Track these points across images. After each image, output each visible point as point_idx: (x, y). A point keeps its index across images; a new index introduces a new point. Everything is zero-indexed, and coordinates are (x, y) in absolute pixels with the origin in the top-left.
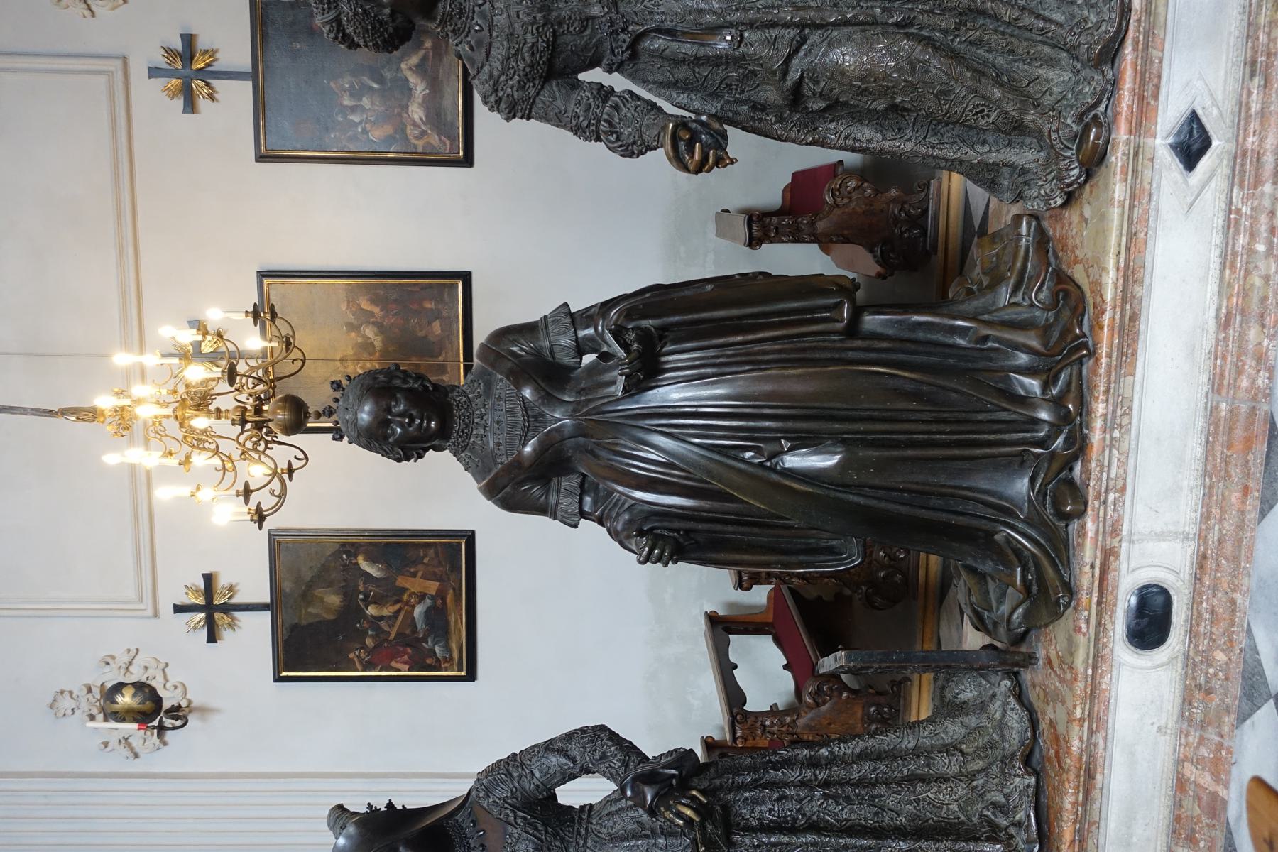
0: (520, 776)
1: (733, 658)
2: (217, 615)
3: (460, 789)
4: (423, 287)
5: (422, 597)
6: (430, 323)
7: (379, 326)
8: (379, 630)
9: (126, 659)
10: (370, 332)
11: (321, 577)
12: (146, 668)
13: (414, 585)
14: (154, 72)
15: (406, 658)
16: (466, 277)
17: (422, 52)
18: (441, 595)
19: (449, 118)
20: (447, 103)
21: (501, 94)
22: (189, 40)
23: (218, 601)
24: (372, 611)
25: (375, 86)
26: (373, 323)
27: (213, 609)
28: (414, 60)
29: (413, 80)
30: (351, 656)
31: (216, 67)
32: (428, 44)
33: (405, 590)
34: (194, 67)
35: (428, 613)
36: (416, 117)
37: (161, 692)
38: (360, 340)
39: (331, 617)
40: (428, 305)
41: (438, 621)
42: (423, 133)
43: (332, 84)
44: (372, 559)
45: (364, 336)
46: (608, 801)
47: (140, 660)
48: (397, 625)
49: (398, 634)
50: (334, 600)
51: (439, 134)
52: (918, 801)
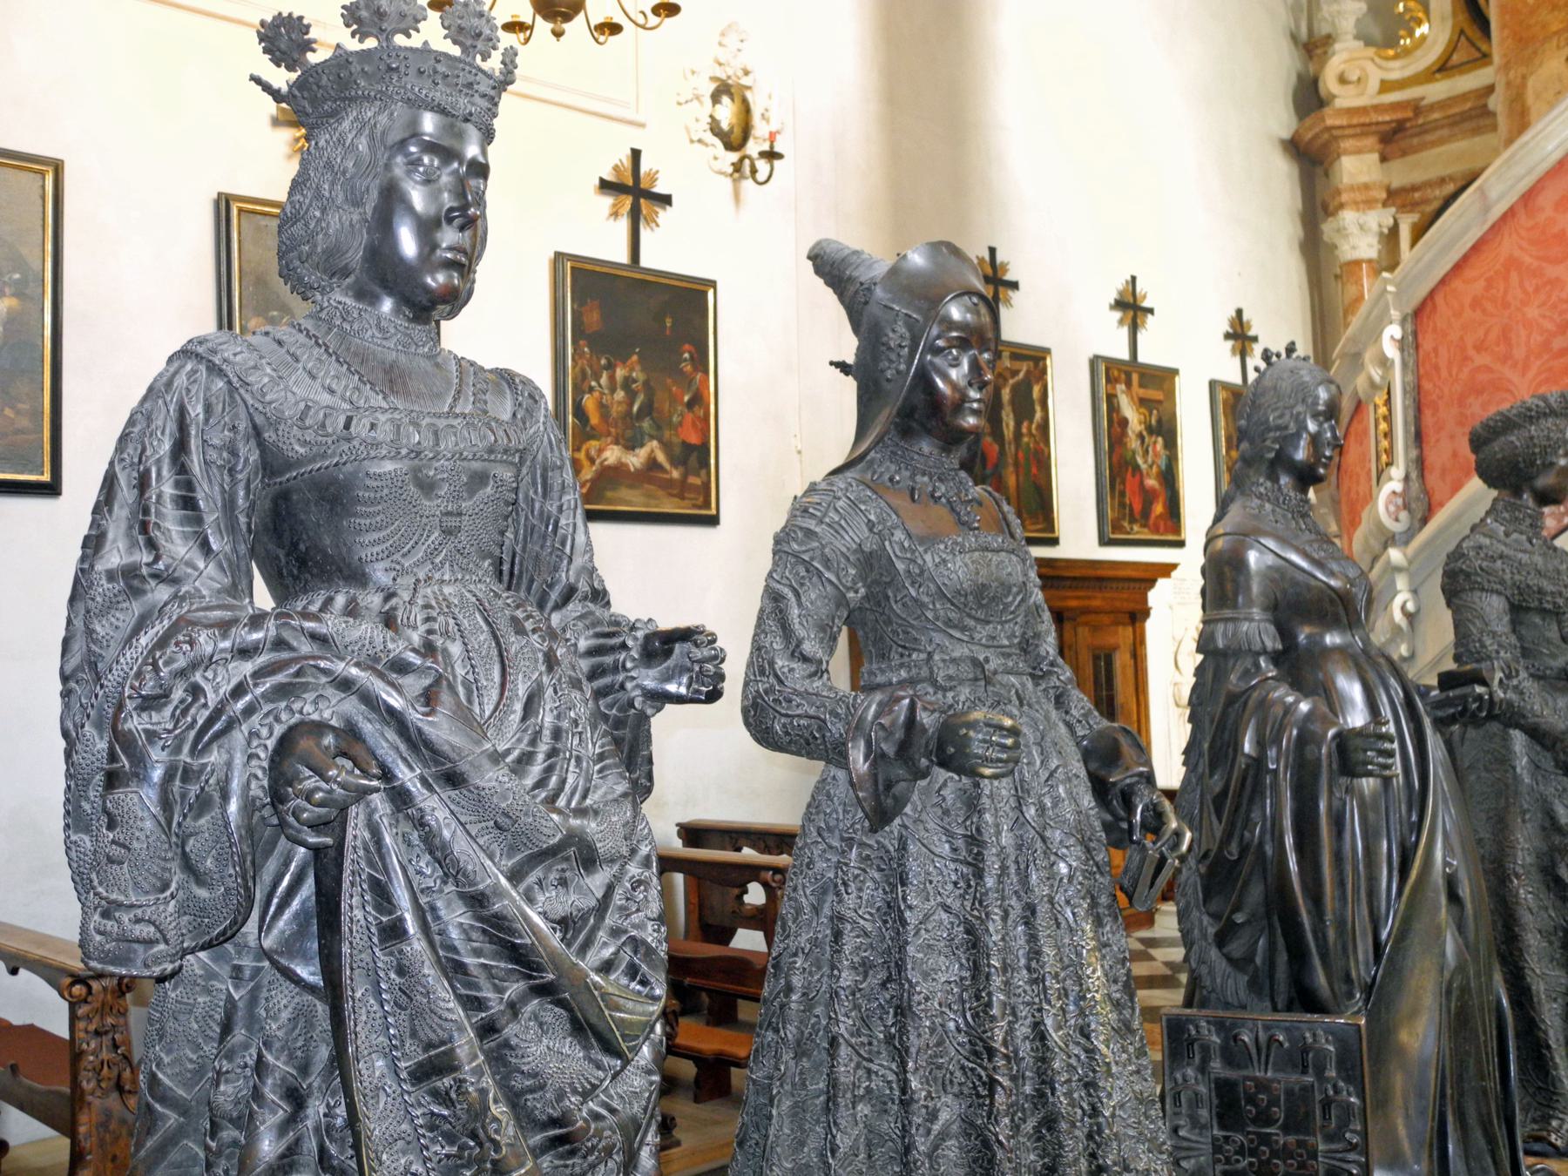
14: (636, 154)
17: (667, 466)
19: (609, 494)
20: (624, 493)
21: (1499, 563)
25: (635, 408)
28: (661, 457)
29: (643, 453)
32: (676, 474)
43: (635, 358)
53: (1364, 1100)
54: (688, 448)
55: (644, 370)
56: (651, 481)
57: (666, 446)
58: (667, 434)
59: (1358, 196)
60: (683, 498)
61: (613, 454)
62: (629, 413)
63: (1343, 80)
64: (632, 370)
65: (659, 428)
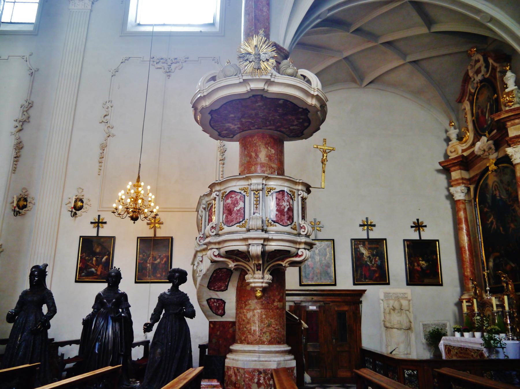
1: (73, 345)
3: (48, 287)
5: (96, 270)
8: (90, 260)
10: (158, 260)
11: (103, 248)
13: (100, 269)
18: (96, 275)
23: (100, 225)
24: (94, 259)
27: (98, 223)
33: (99, 266)
35: (93, 272)
39: (94, 249)
40: (164, 274)
41: (91, 274)
44: (106, 259)
46: (43, 313)
49: (88, 265)
50: (98, 250)
59: (455, 183)
63: (451, 152)
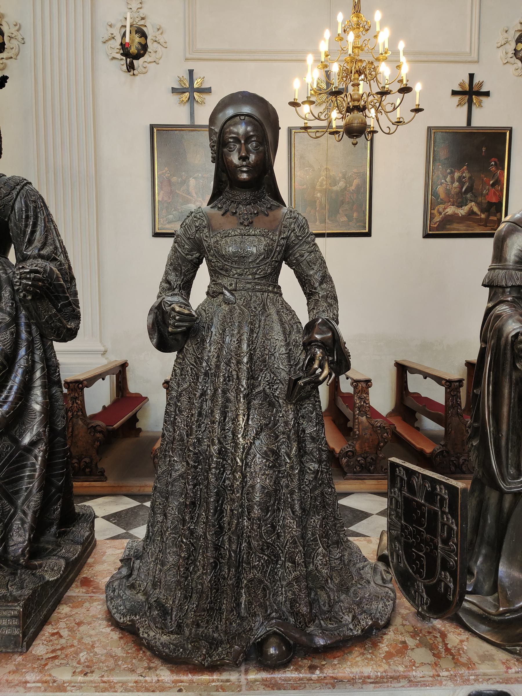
0: (309, 243)
2: (187, 94)
4: (364, 212)
6: (346, 215)
7: (345, 189)
9: (161, 41)
10: (342, 184)
12: (156, 52)
15: (165, 199)
16: (368, 234)
17: (479, 213)
19: (448, 226)
20: (455, 226)
22: (487, 94)
25: (464, 189)
26: (346, 186)
28: (476, 209)
29: (466, 209)
30: (166, 169)
31: (474, 108)
32: (483, 216)
34: (474, 96)
36: (448, 210)
37: (142, 60)
38: (338, 178)
40: (355, 215)
42: (440, 213)
43: (465, 167)
45: (340, 181)
47: (160, 48)
48: (184, 195)
51: (439, 221)
52: (315, 540)
53: (458, 528)
54: (490, 204)
55: (469, 172)
56: (469, 220)
57: (478, 204)
58: (480, 199)
60: (486, 226)
61: (451, 210)
62: (460, 192)
64: (464, 172)
65: (476, 197)
